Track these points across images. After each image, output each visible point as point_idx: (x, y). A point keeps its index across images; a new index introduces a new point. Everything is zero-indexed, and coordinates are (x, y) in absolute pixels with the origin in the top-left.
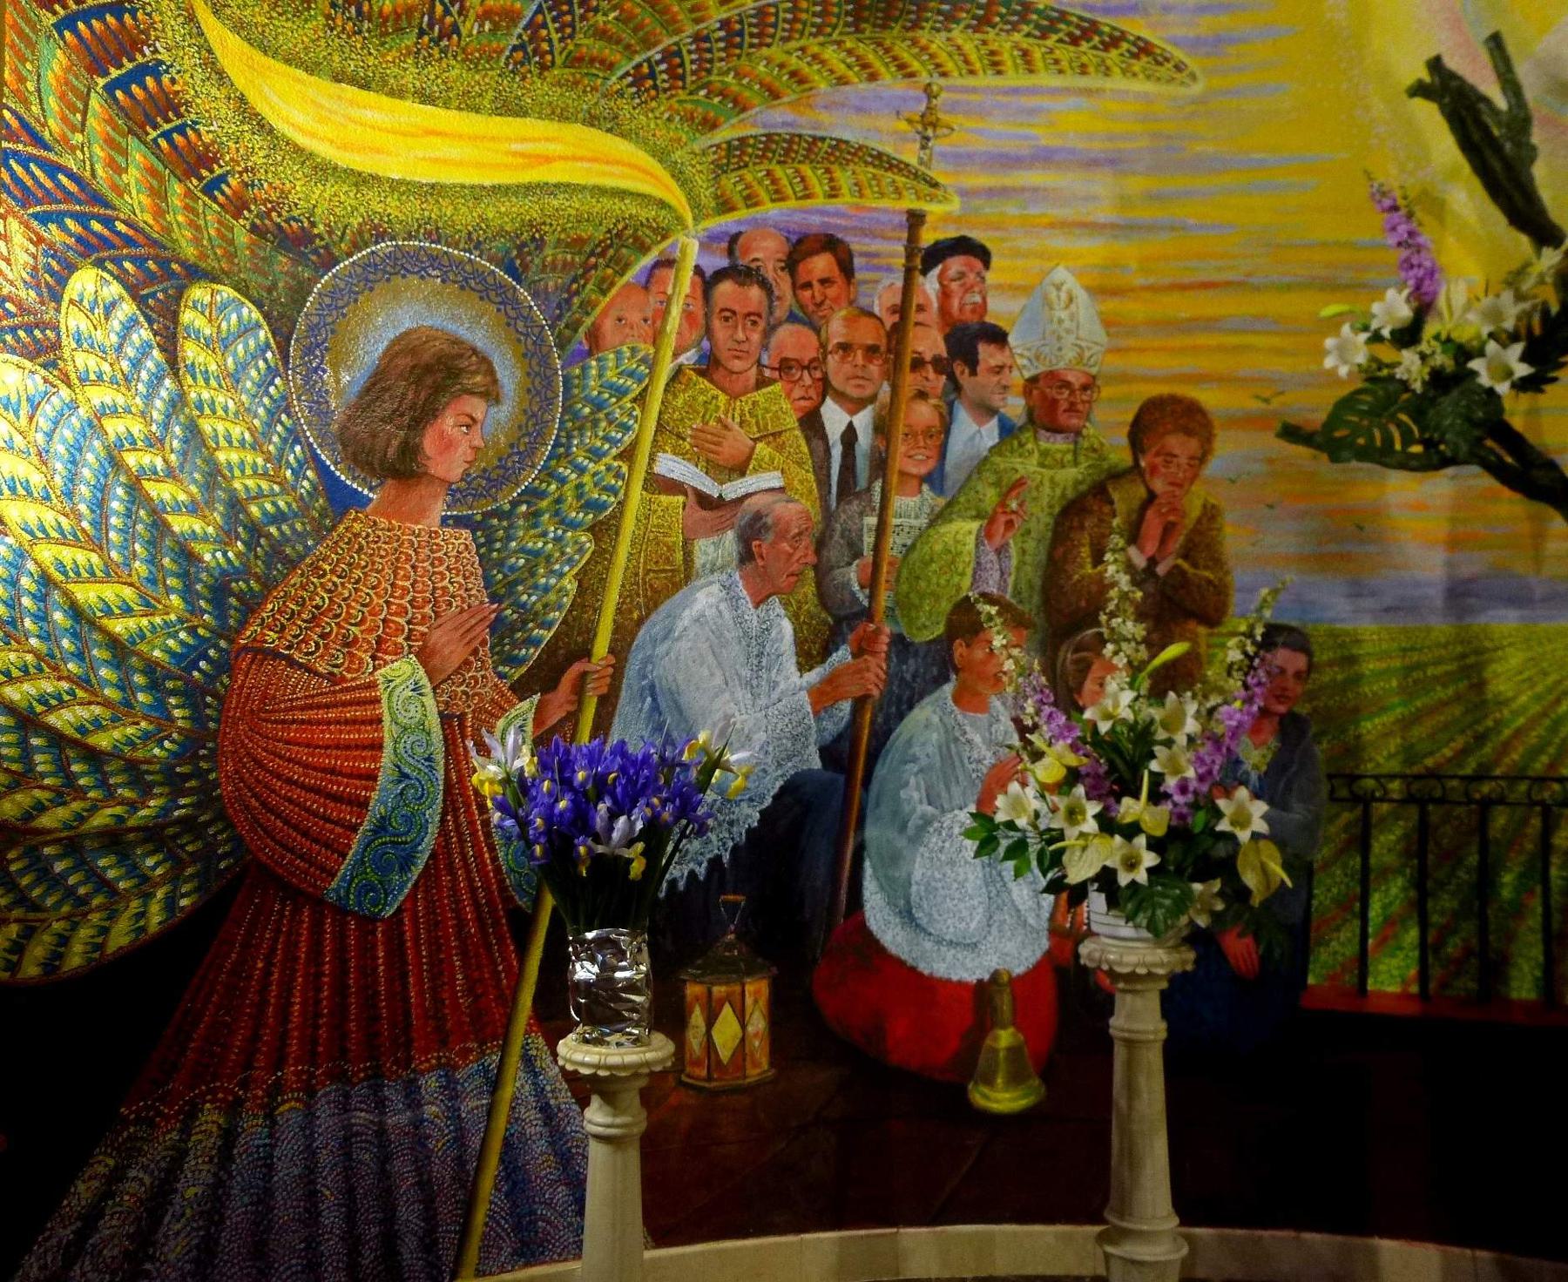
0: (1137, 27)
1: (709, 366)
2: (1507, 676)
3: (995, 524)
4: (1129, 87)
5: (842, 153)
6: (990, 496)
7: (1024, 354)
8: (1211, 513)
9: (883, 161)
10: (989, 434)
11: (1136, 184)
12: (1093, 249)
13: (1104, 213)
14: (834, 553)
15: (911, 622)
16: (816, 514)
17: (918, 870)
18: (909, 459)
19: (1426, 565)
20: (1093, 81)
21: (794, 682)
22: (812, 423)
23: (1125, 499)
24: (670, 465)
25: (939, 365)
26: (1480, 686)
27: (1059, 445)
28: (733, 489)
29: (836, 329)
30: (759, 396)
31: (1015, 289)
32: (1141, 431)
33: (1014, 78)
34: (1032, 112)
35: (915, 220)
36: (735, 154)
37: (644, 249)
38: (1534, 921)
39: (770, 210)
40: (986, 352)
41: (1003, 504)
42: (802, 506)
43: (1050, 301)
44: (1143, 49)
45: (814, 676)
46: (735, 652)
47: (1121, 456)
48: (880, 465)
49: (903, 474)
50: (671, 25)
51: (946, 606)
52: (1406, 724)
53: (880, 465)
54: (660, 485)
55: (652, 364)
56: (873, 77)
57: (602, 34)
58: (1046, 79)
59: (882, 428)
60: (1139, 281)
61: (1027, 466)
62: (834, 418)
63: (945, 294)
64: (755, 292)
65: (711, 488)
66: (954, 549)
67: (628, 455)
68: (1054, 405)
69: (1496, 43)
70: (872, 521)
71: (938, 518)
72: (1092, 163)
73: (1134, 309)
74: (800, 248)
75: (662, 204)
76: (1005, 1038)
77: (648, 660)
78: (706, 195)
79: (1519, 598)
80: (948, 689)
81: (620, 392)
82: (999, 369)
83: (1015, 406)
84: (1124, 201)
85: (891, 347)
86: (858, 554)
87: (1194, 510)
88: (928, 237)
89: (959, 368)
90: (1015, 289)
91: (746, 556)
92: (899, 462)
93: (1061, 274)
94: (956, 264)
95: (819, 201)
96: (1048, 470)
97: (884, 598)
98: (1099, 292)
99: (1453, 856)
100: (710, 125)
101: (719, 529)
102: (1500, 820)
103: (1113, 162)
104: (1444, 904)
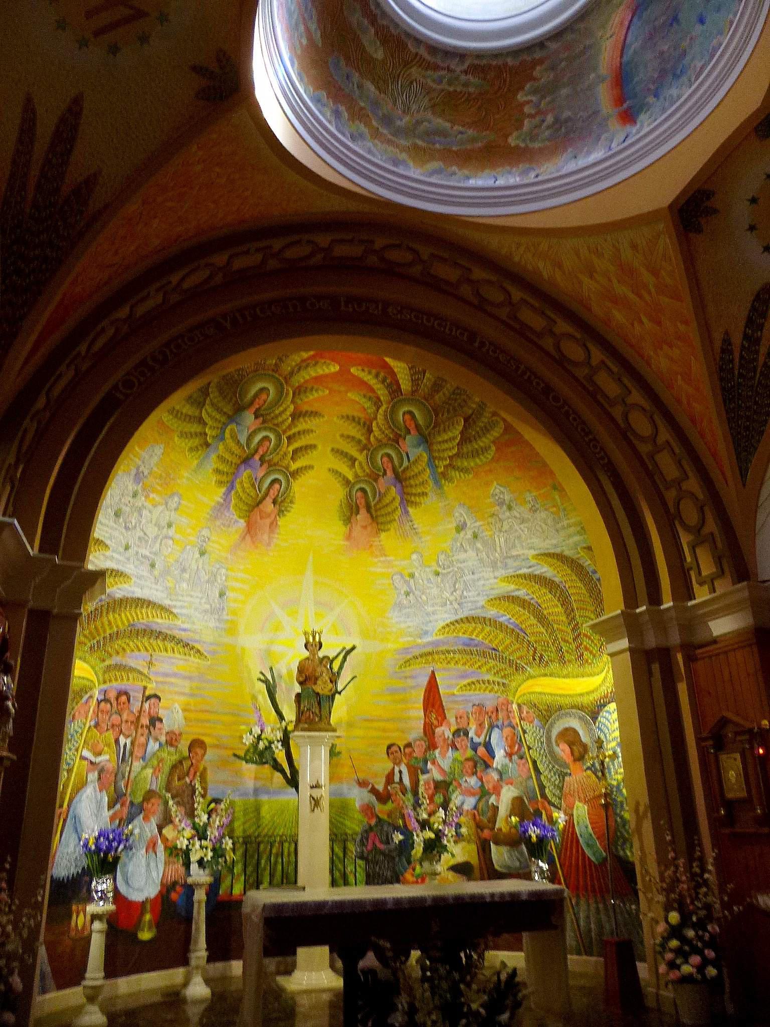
0: (197, 646)
1: (97, 725)
2: (265, 811)
3: (157, 770)
4: (195, 660)
5: (132, 669)
6: (155, 763)
7: (166, 726)
8: (205, 769)
9: (141, 673)
10: (157, 746)
11: (194, 684)
12: (183, 699)
13: (187, 691)
14: (120, 776)
15: (135, 796)
16: (116, 767)
17: (131, 868)
18: (138, 752)
19: (250, 784)
20: (187, 657)
21: (107, 814)
22: (117, 741)
23: (186, 765)
24: (86, 753)
25: (147, 726)
26: (259, 813)
27: (172, 749)
28: (98, 760)
29: (125, 717)
30: (107, 734)
31: (166, 708)
32: (191, 748)
33: (170, 654)
34: (173, 663)
35: (145, 688)
36: (109, 668)
37: (86, 693)
38: (268, 872)
39: (114, 684)
40: (158, 724)
41: (158, 765)
42: (112, 766)
43: (173, 715)
44: (198, 651)
45: (111, 812)
46: (94, 806)
47: (186, 753)
48: (131, 754)
49: (137, 757)
50: (99, 635)
51: (143, 792)
52: (244, 823)
53: (131, 754)
54: (83, 758)
55: (85, 725)
56: (139, 650)
57: (85, 636)
58: (177, 655)
59: (132, 743)
60: (193, 708)
61: (164, 755)
62: (122, 740)
63: (150, 708)
64: (109, 705)
65: (93, 759)
66: (146, 776)
67: (77, 750)
68: (172, 740)
69: (271, 669)
70: (128, 769)
71: (144, 768)
72: (185, 678)
73: (192, 716)
74: (121, 693)
75: (92, 681)
76: (148, 917)
77: (75, 809)
78: (101, 679)
79: (268, 792)
80: (141, 816)
81: (77, 732)
82: (160, 729)
83: (163, 739)
84: (191, 688)
85: (136, 722)
86: (124, 777)
87: (201, 768)
88: (147, 693)
89: (152, 729)
90: (166, 708)
91: (99, 778)
92: (136, 753)
93: (176, 705)
94: (153, 700)
95: (125, 682)
96: (170, 757)
97: (129, 790)
98: (184, 710)
99: (252, 857)
100: (104, 660)
101: (93, 771)
102: (262, 847)
103: (190, 678)
104: (250, 869)
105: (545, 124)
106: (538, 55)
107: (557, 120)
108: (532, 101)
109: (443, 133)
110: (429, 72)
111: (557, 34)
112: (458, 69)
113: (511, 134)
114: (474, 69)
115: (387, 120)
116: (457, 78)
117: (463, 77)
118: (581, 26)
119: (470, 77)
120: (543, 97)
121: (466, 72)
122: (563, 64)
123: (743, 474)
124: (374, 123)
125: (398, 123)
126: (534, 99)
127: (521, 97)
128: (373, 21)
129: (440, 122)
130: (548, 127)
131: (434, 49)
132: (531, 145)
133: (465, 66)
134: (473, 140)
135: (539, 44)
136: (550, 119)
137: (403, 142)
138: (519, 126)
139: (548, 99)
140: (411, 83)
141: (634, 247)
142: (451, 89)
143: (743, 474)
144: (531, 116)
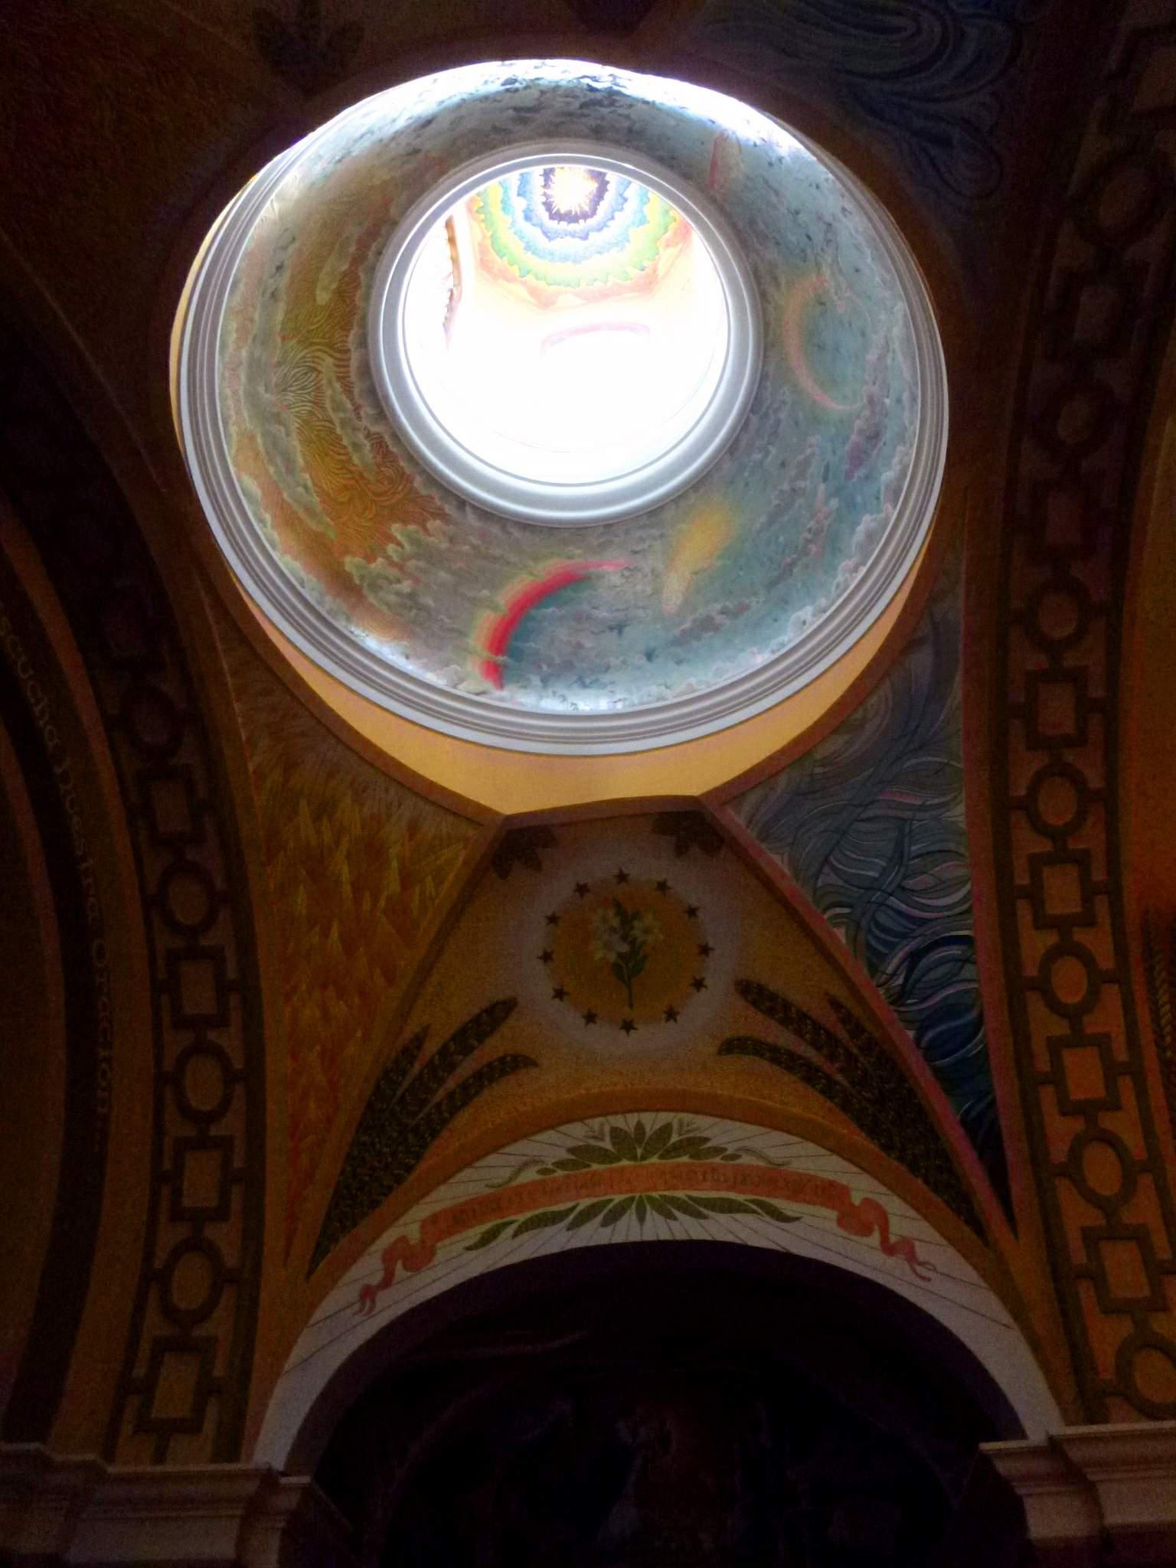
105: (398, 586)
106: (449, 509)
107: (412, 596)
108: (402, 547)
110: (337, 386)
111: (488, 514)
112: (365, 423)
113: (354, 554)
114: (379, 444)
116: (355, 429)
117: (361, 437)
118: (517, 533)
120: (417, 556)
122: (466, 548)
124: (244, 353)
125: (261, 389)
126: (407, 547)
127: (396, 529)
128: (358, 260)
129: (296, 445)
130: (398, 594)
131: (368, 371)
132: (366, 591)
133: (374, 429)
134: (309, 511)
135: (462, 501)
136: (406, 586)
138: (370, 558)
139: (422, 564)
140: (314, 369)
141: (413, 829)
142: (338, 431)
144: (388, 558)
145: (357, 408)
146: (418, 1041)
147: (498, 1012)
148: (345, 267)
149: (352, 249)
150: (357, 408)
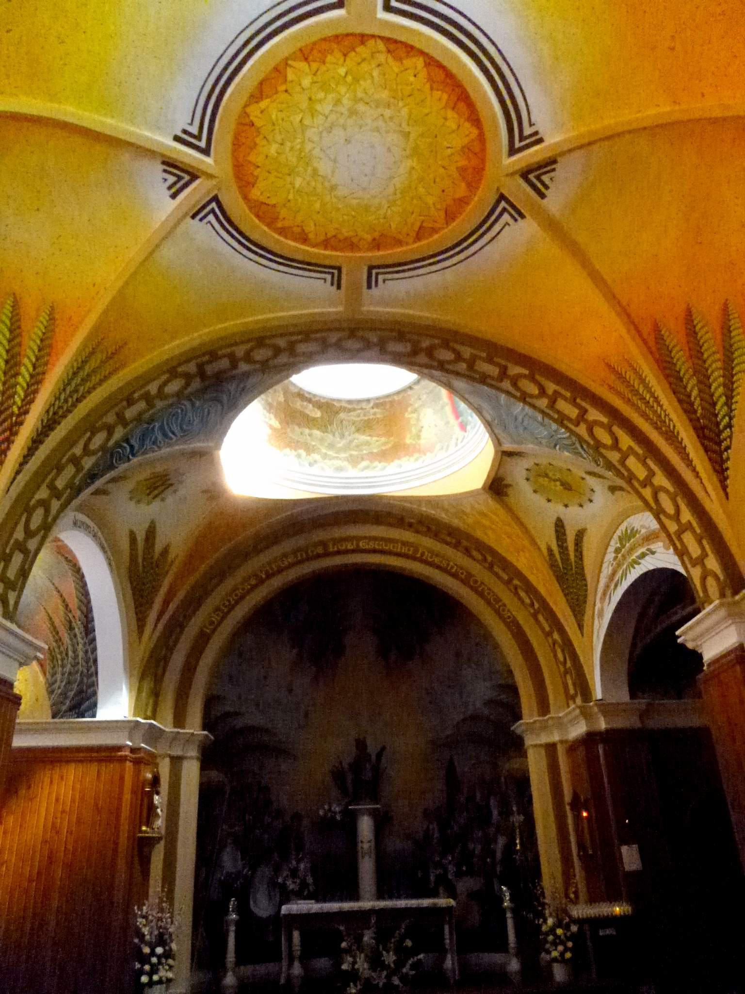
109: (368, 443)
110: (352, 413)
114: (377, 405)
115: (331, 446)
117: (372, 411)
119: (375, 410)
121: (373, 408)
123: (581, 627)
128: (309, 401)
133: (372, 404)
134: (385, 444)
137: (343, 455)
140: (342, 422)
142: (366, 418)
143: (581, 627)
145: (362, 409)
146: (550, 550)
147: (559, 525)
148: (311, 406)
149: (305, 403)
150: (362, 409)
